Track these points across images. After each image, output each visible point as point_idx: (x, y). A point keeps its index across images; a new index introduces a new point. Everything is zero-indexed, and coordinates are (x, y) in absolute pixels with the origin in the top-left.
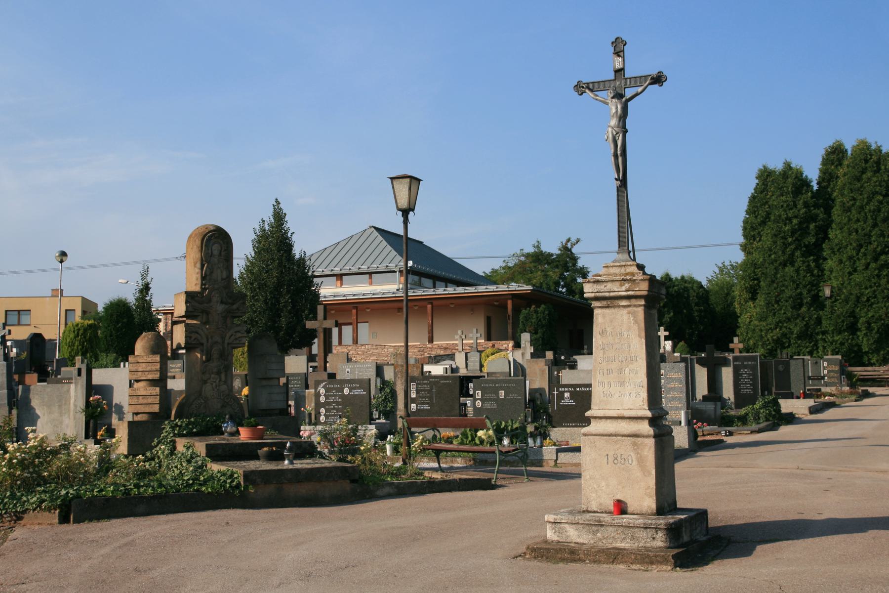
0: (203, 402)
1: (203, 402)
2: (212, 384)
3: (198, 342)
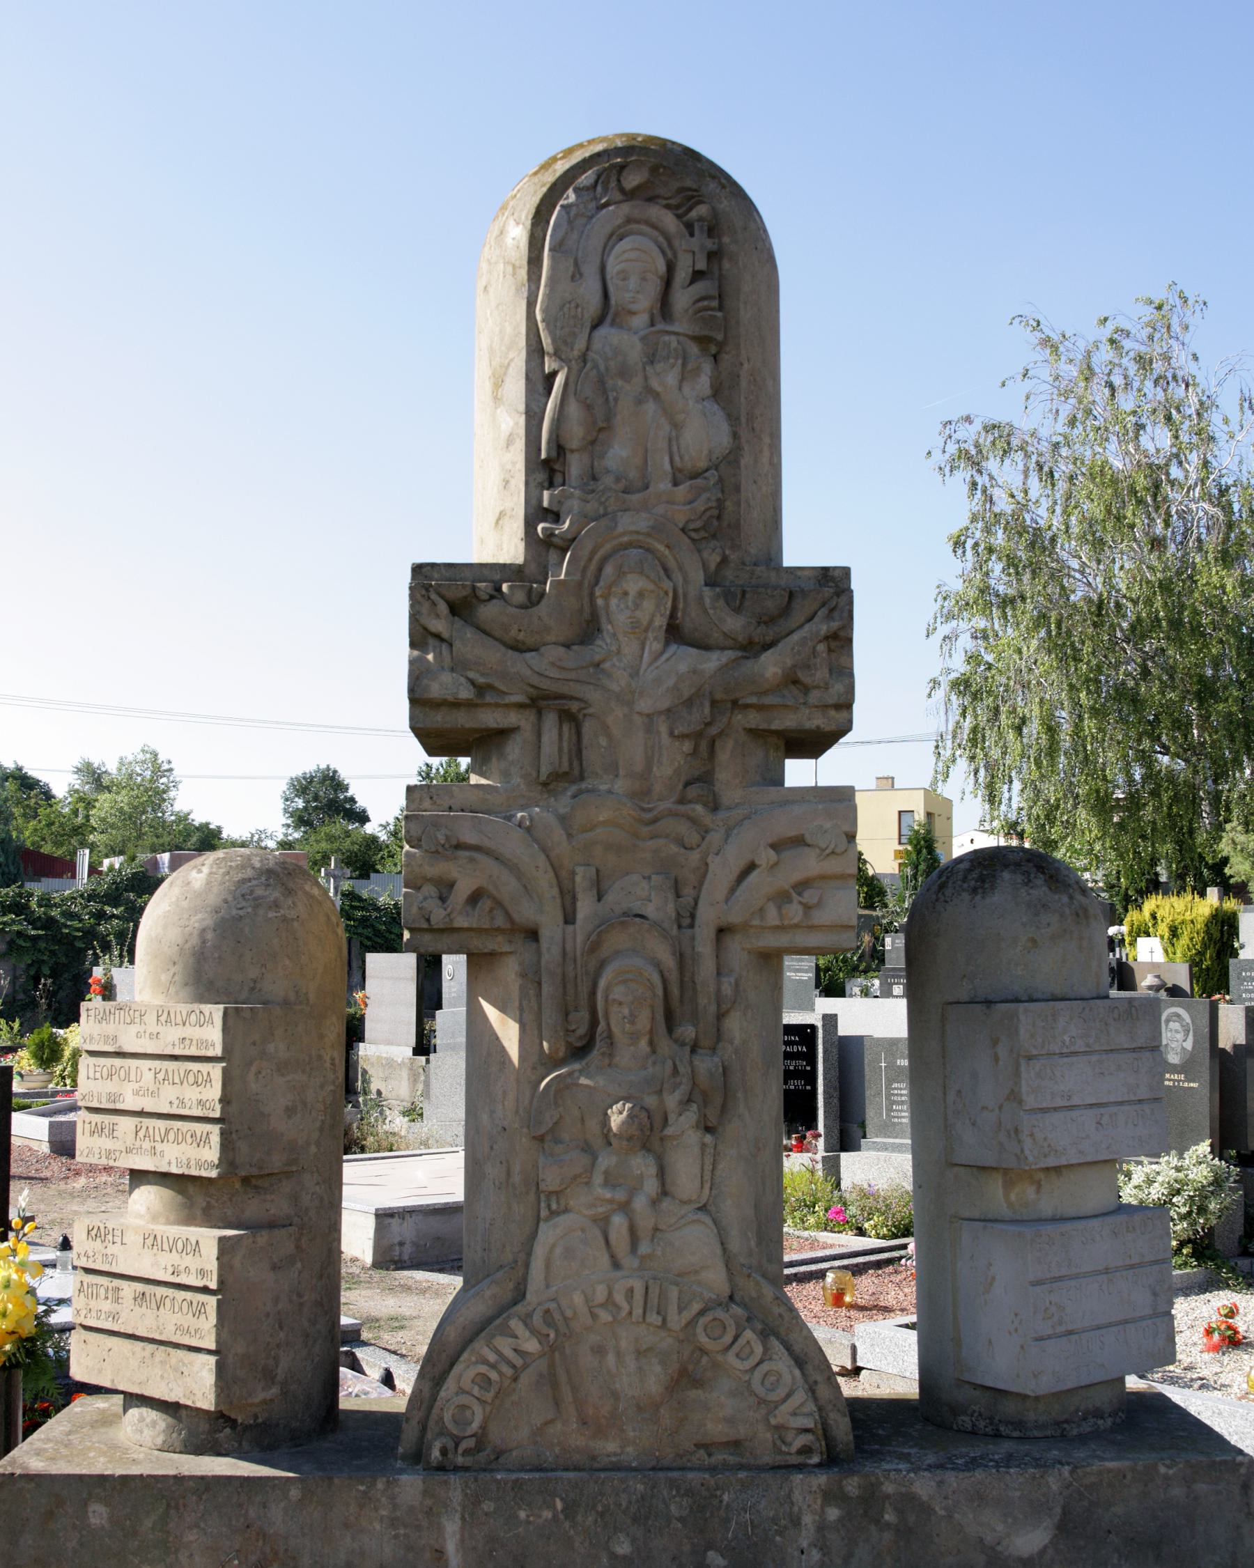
0: (532, 1346)
1: (532, 1346)
2: (603, 1223)
3: (500, 921)
